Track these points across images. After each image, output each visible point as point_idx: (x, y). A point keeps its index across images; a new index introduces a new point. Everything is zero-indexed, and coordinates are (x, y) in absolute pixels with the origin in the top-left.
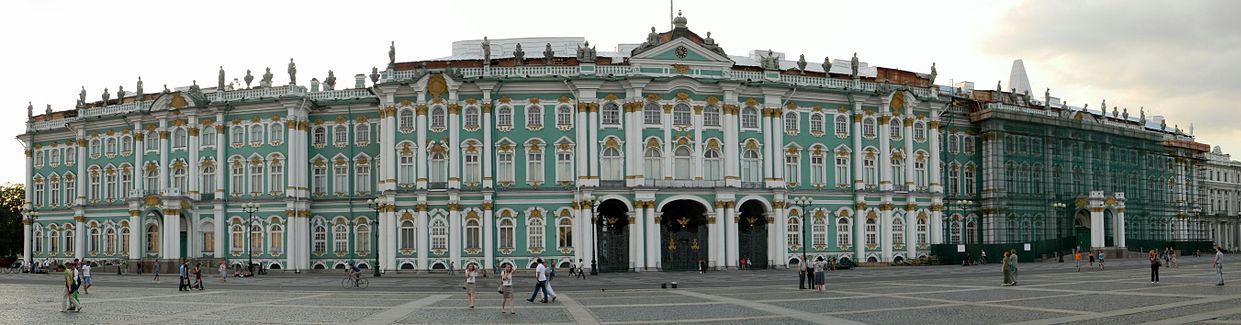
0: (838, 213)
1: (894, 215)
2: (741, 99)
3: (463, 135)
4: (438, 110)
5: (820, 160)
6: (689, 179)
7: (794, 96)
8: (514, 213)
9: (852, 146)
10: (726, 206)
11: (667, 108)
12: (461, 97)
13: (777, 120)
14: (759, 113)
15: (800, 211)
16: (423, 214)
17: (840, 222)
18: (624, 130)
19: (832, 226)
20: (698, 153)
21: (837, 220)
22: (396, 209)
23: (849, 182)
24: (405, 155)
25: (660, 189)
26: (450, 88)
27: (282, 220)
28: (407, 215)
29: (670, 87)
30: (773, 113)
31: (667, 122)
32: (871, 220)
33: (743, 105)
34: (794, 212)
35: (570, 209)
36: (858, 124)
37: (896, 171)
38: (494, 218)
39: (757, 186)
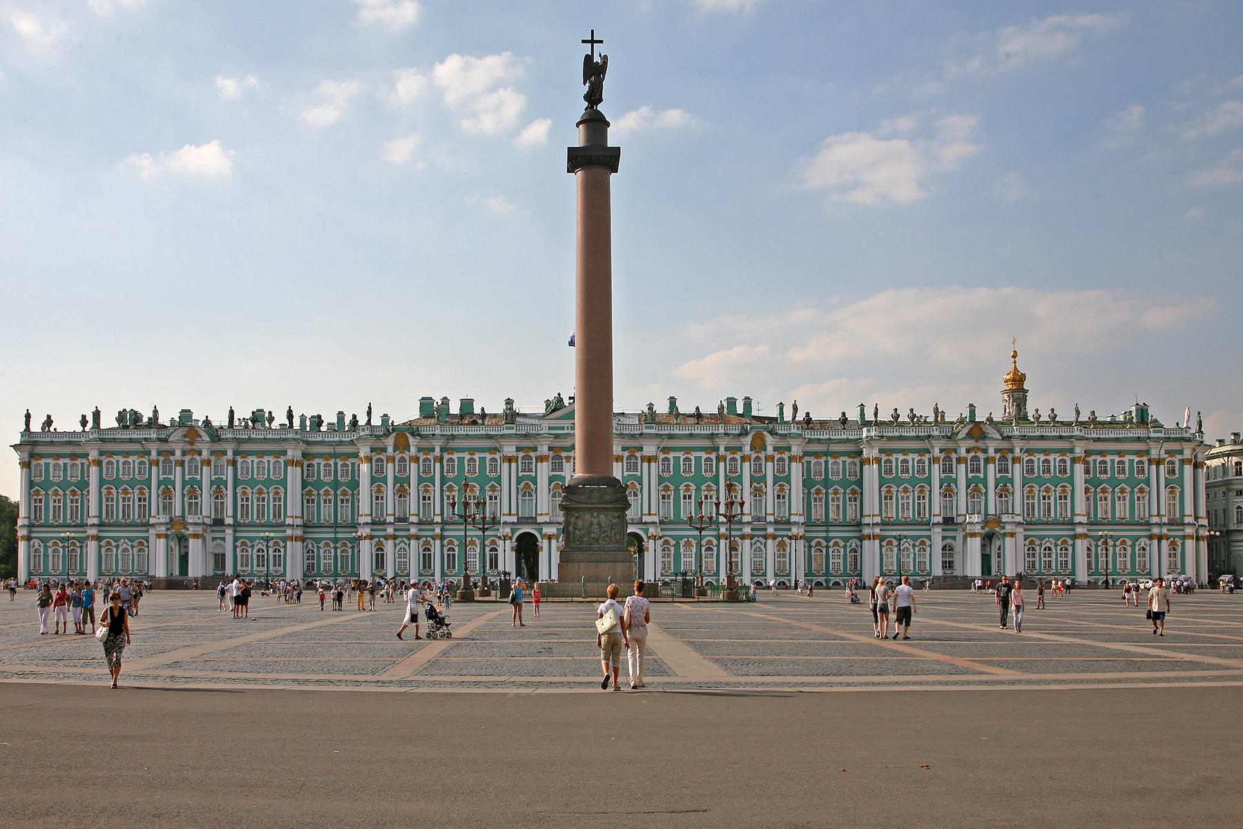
3: (420, 480)
5: (690, 497)
9: (717, 484)
22: (371, 537)
24: (378, 496)
27: (282, 544)
28: (379, 543)
37: (757, 505)
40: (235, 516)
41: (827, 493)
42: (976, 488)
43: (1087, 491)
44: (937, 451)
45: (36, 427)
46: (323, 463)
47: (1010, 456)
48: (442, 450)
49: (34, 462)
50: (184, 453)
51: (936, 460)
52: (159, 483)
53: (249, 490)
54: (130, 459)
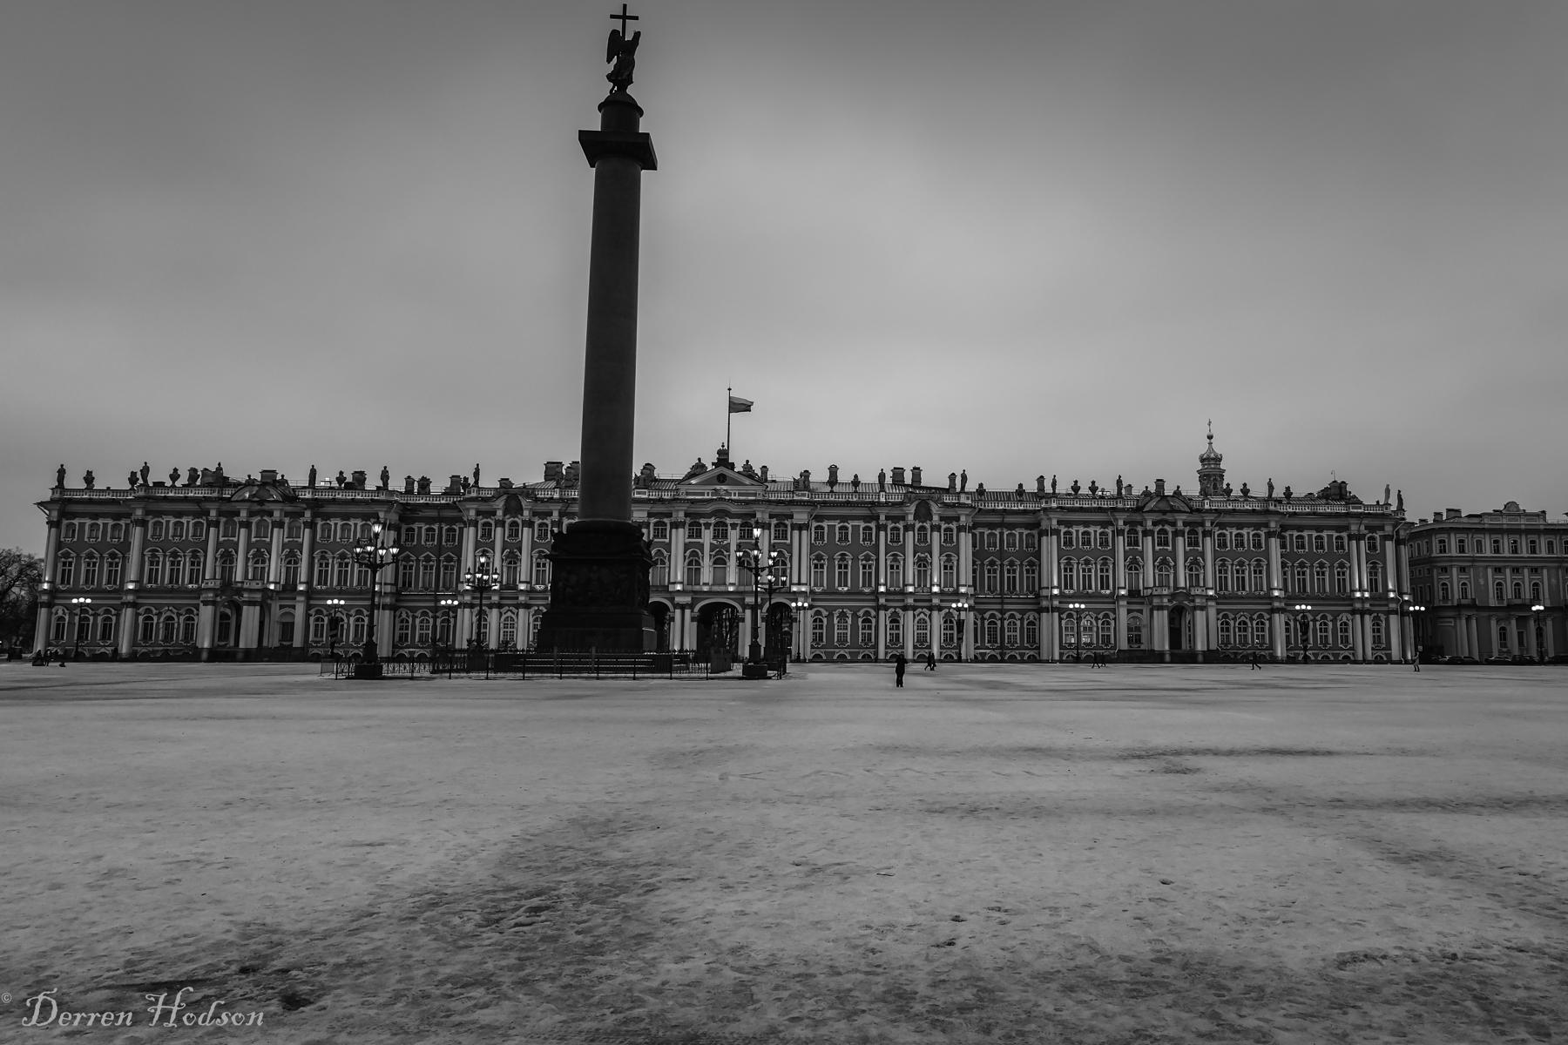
0: (861, 613)
2: (771, 516)
4: (514, 524)
7: (819, 511)
9: (877, 554)
11: (707, 526)
12: (535, 514)
13: (804, 533)
15: (825, 613)
16: (495, 611)
19: (854, 626)
25: (695, 592)
29: (709, 509)
30: (800, 528)
31: (707, 537)
33: (774, 521)
36: (882, 534)
40: (309, 583)
41: (1002, 566)
42: (1164, 563)
43: (1284, 565)
44: (1121, 523)
45: (74, 482)
46: (425, 527)
47: (1200, 530)
48: (562, 514)
49: (65, 522)
50: (251, 514)
51: (1120, 532)
52: (218, 545)
53: (329, 555)
54: (184, 520)
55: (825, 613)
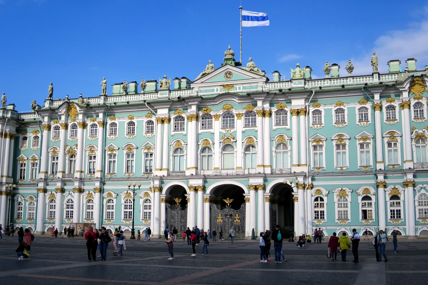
1: (419, 191)
6: (233, 169)
8: (114, 195)
10: (256, 188)
13: (302, 117)
14: (289, 114)
17: (364, 199)
18: (186, 135)
19: (354, 203)
20: (239, 148)
21: (360, 198)
23: (372, 164)
26: (79, 112)
30: (298, 113)
32: (395, 197)
34: (319, 191)
35: (149, 192)
36: (377, 112)
38: (102, 199)
39: (284, 172)
55: (325, 192)
